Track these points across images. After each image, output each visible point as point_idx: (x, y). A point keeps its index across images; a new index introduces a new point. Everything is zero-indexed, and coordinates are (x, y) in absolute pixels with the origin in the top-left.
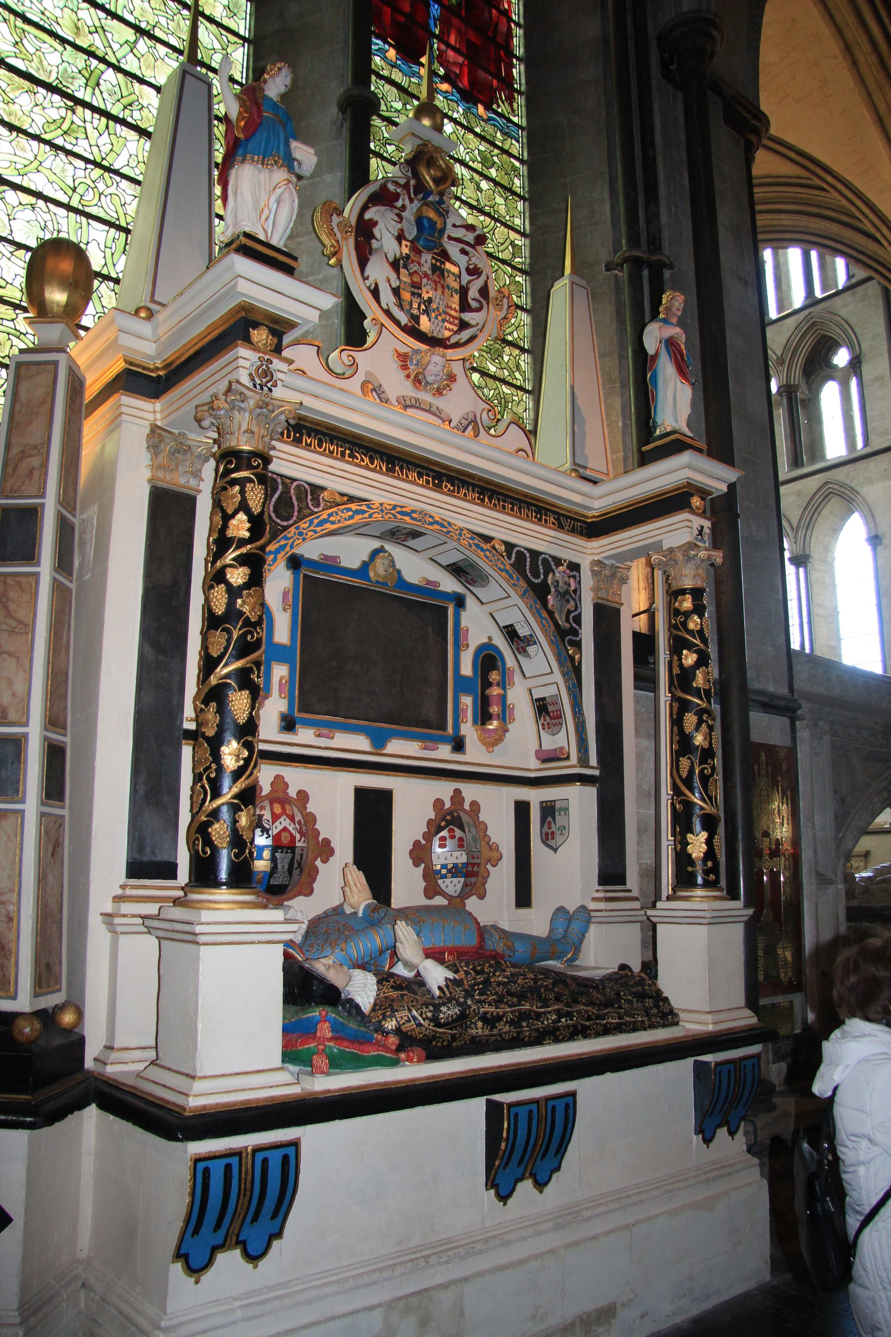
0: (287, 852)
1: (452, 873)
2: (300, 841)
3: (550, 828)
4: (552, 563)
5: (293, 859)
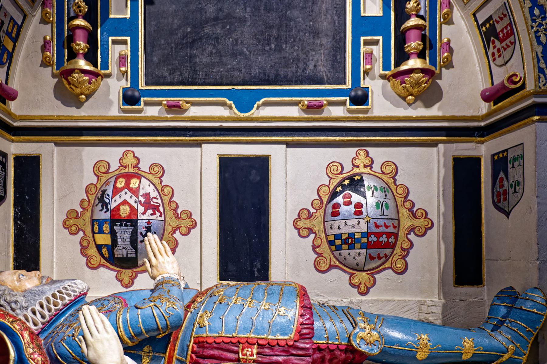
0: (126, 225)
1: (349, 245)
2: (144, 214)
3: (502, 186)
5: (134, 233)
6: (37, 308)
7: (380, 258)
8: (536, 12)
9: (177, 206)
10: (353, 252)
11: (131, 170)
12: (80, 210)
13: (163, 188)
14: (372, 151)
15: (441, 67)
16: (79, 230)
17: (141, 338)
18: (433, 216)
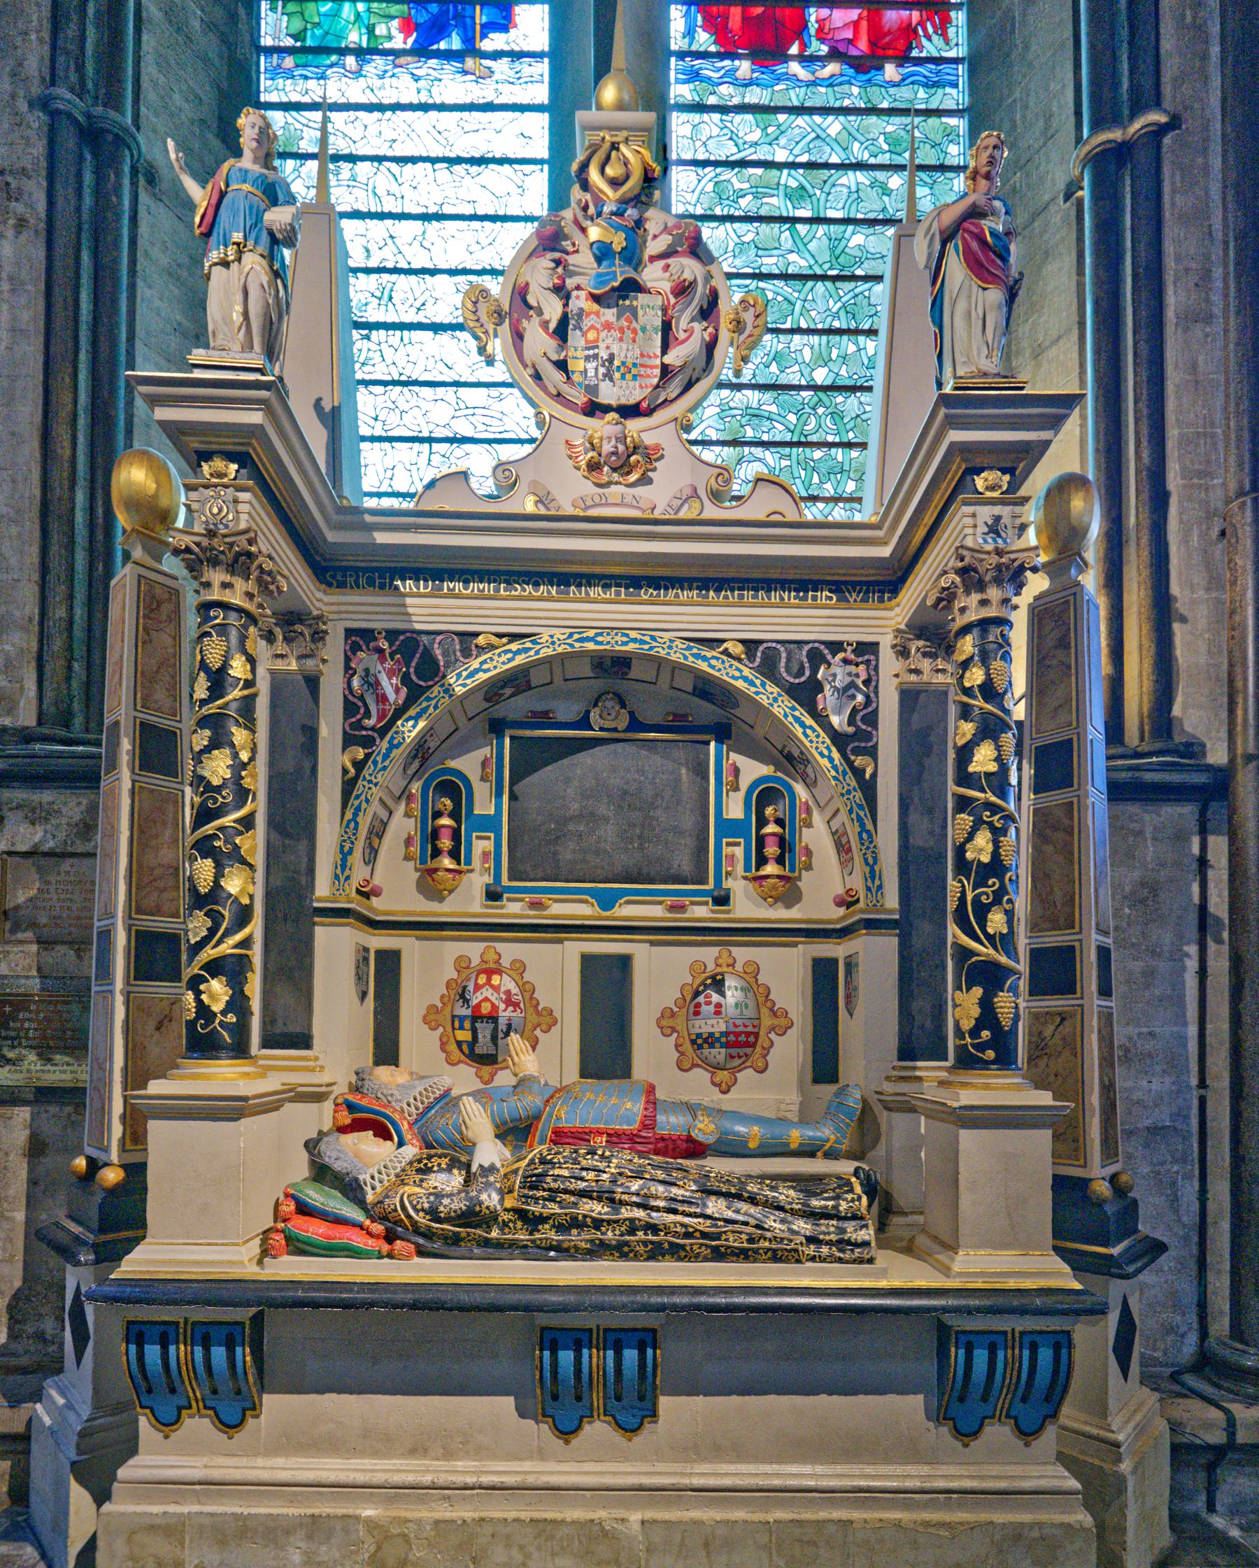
4: (826, 652)
6: (412, 1100)
7: (740, 1057)
8: (865, 836)
10: (713, 1051)
11: (493, 966)
12: (440, 1005)
13: (524, 984)
14: (734, 950)
18: (792, 1015)
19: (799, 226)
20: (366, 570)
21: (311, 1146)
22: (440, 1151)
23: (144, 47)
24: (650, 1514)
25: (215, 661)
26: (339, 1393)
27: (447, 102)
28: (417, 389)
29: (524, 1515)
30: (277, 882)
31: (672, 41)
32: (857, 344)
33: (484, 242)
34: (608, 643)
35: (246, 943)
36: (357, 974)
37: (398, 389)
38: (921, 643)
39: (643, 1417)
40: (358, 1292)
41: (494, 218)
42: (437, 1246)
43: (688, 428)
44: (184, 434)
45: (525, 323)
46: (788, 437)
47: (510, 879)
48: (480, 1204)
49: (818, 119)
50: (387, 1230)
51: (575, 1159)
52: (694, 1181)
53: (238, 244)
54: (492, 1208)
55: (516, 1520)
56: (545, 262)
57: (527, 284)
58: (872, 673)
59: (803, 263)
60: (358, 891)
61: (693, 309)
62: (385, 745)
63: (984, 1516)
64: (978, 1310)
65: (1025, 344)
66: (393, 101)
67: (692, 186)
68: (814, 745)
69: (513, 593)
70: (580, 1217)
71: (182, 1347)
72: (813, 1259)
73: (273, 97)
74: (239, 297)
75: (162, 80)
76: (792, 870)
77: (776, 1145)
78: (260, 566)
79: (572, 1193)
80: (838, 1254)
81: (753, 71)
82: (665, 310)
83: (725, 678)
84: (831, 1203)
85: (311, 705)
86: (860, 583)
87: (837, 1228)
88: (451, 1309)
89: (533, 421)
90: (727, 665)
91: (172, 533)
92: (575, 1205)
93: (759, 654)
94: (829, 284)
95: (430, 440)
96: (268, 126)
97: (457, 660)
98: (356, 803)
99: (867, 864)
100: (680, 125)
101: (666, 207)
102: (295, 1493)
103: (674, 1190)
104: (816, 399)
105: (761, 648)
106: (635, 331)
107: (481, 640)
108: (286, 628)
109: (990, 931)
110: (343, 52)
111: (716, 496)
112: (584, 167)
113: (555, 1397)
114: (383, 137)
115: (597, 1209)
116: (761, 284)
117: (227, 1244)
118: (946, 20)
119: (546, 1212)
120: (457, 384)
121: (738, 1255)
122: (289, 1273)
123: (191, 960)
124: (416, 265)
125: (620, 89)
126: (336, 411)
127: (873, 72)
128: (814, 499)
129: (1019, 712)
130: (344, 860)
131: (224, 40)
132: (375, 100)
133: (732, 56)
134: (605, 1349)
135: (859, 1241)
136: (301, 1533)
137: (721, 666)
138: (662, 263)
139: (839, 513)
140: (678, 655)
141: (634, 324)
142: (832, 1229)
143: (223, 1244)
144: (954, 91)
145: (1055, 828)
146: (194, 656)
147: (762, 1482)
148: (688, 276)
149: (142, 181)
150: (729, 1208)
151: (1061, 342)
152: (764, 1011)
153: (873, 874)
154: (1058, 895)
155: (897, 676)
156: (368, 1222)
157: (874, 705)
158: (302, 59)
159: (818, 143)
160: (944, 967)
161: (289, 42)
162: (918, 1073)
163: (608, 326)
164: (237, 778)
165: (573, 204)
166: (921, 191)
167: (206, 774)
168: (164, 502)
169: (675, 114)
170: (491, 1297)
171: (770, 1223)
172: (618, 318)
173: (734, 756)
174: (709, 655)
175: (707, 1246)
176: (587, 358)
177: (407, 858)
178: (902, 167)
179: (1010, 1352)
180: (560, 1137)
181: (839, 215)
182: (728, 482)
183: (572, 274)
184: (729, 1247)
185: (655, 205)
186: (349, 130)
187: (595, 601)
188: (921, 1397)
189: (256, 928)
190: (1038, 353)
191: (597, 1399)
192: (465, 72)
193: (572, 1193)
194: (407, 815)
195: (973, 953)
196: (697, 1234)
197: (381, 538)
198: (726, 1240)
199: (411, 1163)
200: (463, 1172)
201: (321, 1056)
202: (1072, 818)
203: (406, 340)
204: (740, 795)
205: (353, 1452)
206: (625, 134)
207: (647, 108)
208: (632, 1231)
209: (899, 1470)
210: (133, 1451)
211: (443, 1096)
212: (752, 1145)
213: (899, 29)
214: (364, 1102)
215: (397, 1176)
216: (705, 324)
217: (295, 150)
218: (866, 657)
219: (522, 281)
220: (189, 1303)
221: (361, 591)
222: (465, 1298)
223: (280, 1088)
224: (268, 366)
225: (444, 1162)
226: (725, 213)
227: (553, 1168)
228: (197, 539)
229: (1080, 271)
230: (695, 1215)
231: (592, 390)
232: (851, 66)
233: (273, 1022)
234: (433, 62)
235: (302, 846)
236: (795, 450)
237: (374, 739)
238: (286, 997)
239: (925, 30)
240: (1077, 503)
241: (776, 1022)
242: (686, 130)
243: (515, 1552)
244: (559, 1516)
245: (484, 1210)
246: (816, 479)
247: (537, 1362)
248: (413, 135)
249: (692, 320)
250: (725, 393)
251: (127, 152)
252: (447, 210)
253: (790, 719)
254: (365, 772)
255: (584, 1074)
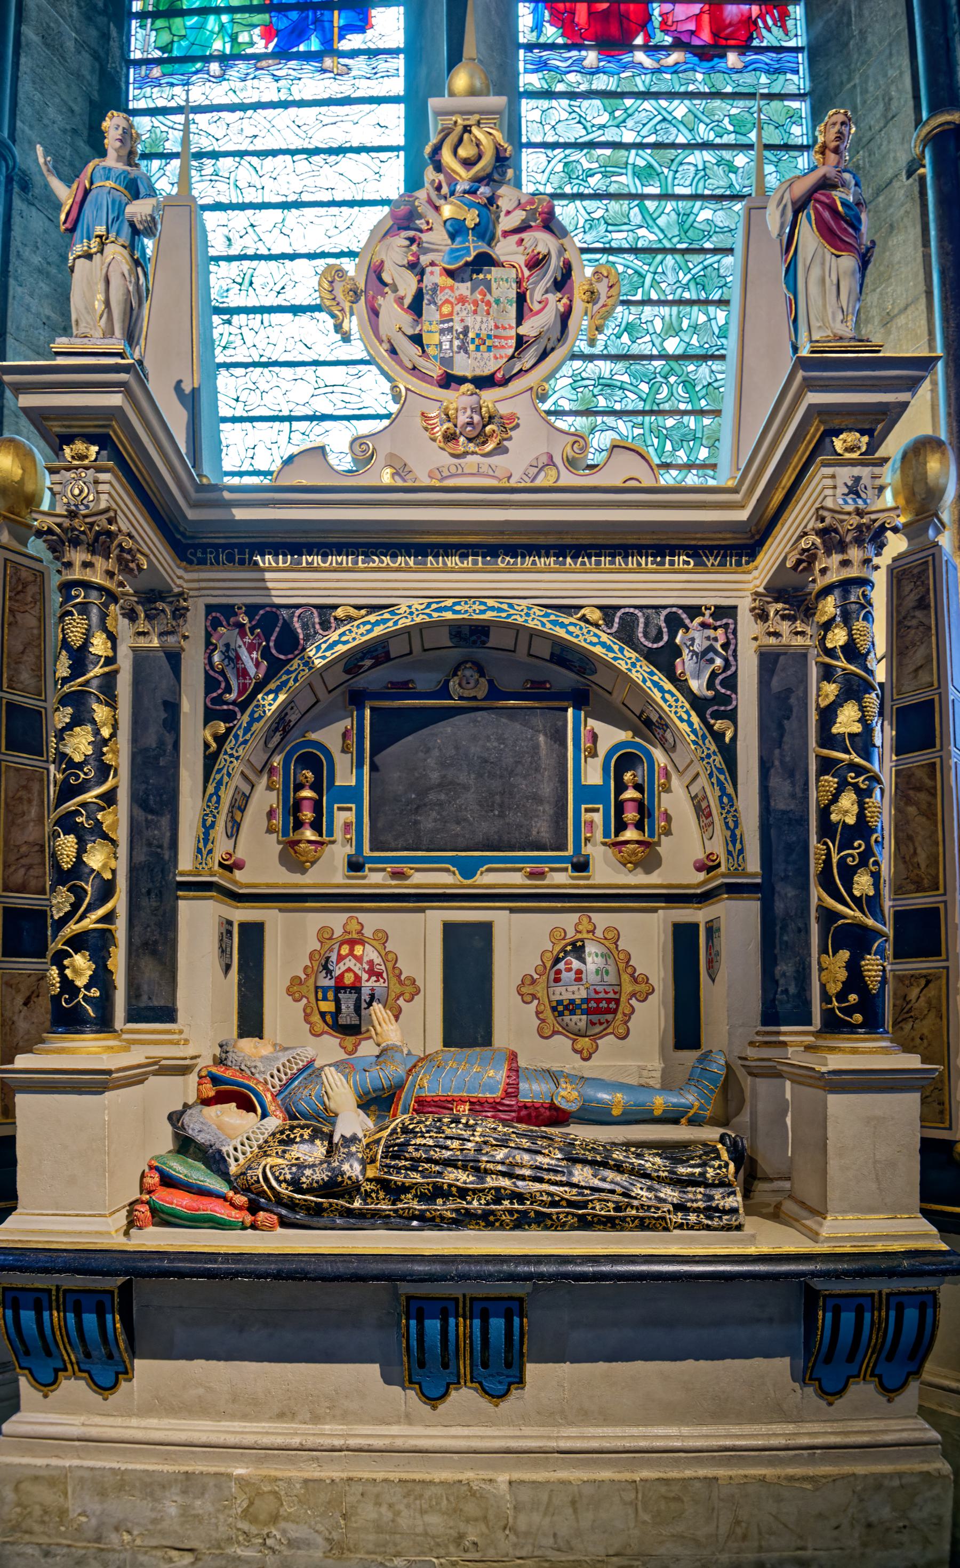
4: (684, 616)
5: (358, 1000)
6: (275, 1072)
7: (601, 1024)
9: (401, 973)
10: (574, 1018)
11: (355, 936)
12: (303, 976)
13: (386, 954)
14: (593, 916)
15: (659, 836)
16: (303, 996)
17: (369, 1097)
18: (653, 981)
19: (648, 203)
20: (225, 546)
21: (175, 1118)
22: (303, 1122)
23: (22, 68)
24: (517, 1475)
25: (76, 639)
26: (207, 1359)
27: (305, 98)
28: (276, 369)
29: (394, 1476)
30: (141, 858)
31: (521, 35)
32: (707, 314)
33: (342, 227)
34: (466, 612)
35: (109, 918)
36: (221, 946)
37: (259, 370)
38: (780, 606)
39: (510, 1384)
40: (222, 1263)
41: (351, 204)
42: (300, 1216)
43: (543, 398)
44: (47, 419)
45: (380, 300)
46: (640, 406)
47: (372, 850)
48: (342, 1174)
49: (664, 103)
50: (250, 1200)
51: (440, 1128)
52: (560, 1150)
53: (100, 237)
54: (354, 1178)
55: (385, 1480)
56: (400, 241)
57: (382, 262)
58: (731, 636)
59: (653, 237)
60: (221, 865)
61: (547, 281)
62: (246, 718)
63: (847, 1469)
64: (846, 1273)
65: (874, 312)
66: (254, 100)
67: (542, 168)
68: (673, 709)
69: (371, 565)
70: (445, 1187)
71: (55, 1314)
72: (680, 1226)
73: (142, 104)
74: (101, 286)
75: (37, 97)
76: (652, 835)
77: (638, 1112)
78: (120, 545)
79: (436, 1162)
80: (706, 1222)
81: (600, 60)
82: (519, 283)
83: (583, 644)
84: (698, 1170)
85: (173, 680)
86: (719, 547)
87: (704, 1195)
88: (314, 1279)
89: (390, 397)
90: (585, 631)
91: (35, 515)
92: (440, 1174)
93: (617, 620)
94: (678, 257)
95: (290, 419)
96: (131, 126)
97: (316, 633)
98: (218, 777)
99: (728, 827)
100: (529, 110)
101: (518, 185)
102: (168, 1452)
103: (540, 1158)
104: (667, 368)
105: (619, 614)
106: (488, 304)
107: (340, 613)
108: (148, 606)
109: (857, 893)
110: (207, 59)
111: (572, 463)
112: (437, 149)
113: (422, 1364)
114: (245, 133)
115: (463, 1178)
116: (612, 258)
117: (94, 1216)
118: (784, 15)
119: (408, 1181)
120: (316, 363)
121: (604, 1224)
122: (155, 1243)
123: (55, 936)
124: (276, 251)
125: (472, 77)
126: (195, 392)
127: (716, 60)
128: (667, 466)
129: (880, 674)
130: (207, 834)
131: (96, 56)
132: (237, 101)
133: (579, 47)
134: (471, 1318)
135: (727, 1206)
136: (175, 1489)
137: (578, 632)
138: (516, 237)
139: (692, 479)
140: (536, 622)
141: (488, 297)
142: (700, 1196)
143: (90, 1216)
144: (795, 78)
145: (918, 789)
146: (57, 636)
147: (628, 1444)
148: (541, 248)
149: (16, 189)
150: (595, 1176)
151: (909, 311)
152: (625, 978)
153: (734, 837)
154: (922, 858)
155: (756, 639)
156: (231, 1194)
157: (733, 669)
158: (168, 68)
159: (664, 125)
160: (807, 930)
161: (157, 54)
162: (782, 1038)
163: (462, 300)
164: (99, 755)
165: (427, 185)
166: (769, 168)
167: (68, 751)
168: (29, 487)
169: (524, 101)
170: (354, 1267)
171: (636, 1191)
172: (473, 291)
173: (591, 722)
174: (566, 621)
175: (574, 1215)
176: (442, 332)
177: (270, 830)
178: (750, 147)
179: (876, 1313)
180: (422, 1105)
181: (687, 191)
182: (584, 449)
183: (426, 251)
184: (595, 1215)
185: (508, 183)
186: (212, 129)
187: (452, 571)
188: (787, 1360)
189: (119, 902)
190: (887, 320)
191: (464, 1368)
192: (324, 71)
193: (436, 1162)
194: (270, 788)
195: (839, 916)
196: (564, 1203)
197: (240, 514)
198: (593, 1208)
199: (273, 1134)
200: (326, 1143)
201: (186, 1030)
202: (934, 779)
203: (266, 323)
204: (599, 761)
205: (223, 1415)
206: (477, 117)
207: (499, 93)
208: (498, 1201)
209: (764, 1429)
210: (16, 1408)
211: (305, 1068)
212: (616, 1112)
213: (740, 21)
214: (228, 1074)
215: (260, 1147)
216: (559, 295)
217: (161, 150)
218: (724, 621)
219: (376, 260)
220: (59, 1272)
221: (221, 567)
222: (327, 1268)
223: (143, 1061)
224: (128, 350)
225: (307, 1133)
226: (575, 191)
227: (415, 1137)
228: (59, 520)
229: (926, 243)
230: (561, 1184)
231: (447, 362)
232: (695, 55)
233: (138, 996)
234: (293, 64)
235: (165, 821)
236: (647, 418)
237: (235, 713)
238: (150, 970)
239: (765, 22)
240: (933, 465)
241: (638, 988)
242: (536, 116)
243: (384, 1509)
244: (428, 1477)
245: (346, 1180)
246: (669, 446)
247: (404, 1330)
248: (272, 130)
249: (547, 292)
250: (577, 364)
251: (3, 164)
252: (306, 198)
253: (649, 684)
254: (227, 747)
255: (448, 1041)
